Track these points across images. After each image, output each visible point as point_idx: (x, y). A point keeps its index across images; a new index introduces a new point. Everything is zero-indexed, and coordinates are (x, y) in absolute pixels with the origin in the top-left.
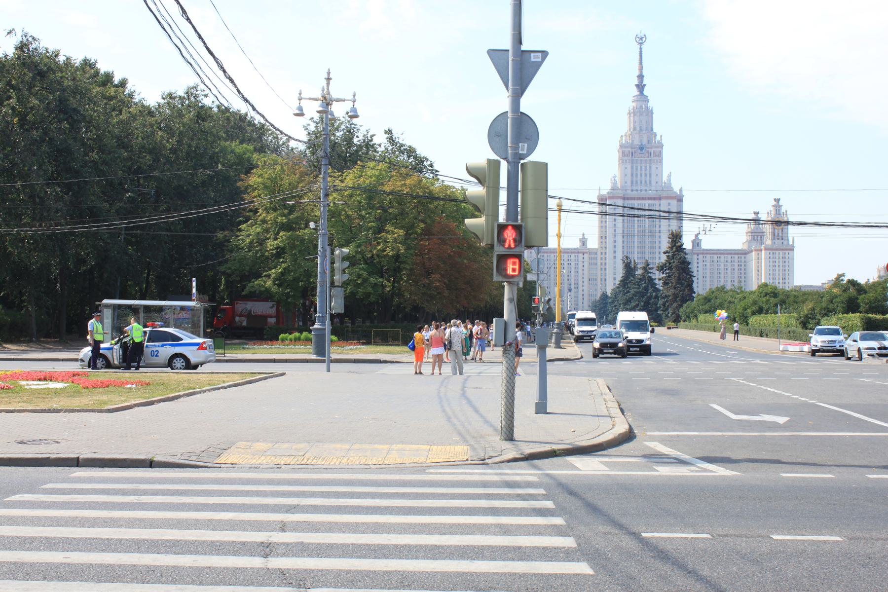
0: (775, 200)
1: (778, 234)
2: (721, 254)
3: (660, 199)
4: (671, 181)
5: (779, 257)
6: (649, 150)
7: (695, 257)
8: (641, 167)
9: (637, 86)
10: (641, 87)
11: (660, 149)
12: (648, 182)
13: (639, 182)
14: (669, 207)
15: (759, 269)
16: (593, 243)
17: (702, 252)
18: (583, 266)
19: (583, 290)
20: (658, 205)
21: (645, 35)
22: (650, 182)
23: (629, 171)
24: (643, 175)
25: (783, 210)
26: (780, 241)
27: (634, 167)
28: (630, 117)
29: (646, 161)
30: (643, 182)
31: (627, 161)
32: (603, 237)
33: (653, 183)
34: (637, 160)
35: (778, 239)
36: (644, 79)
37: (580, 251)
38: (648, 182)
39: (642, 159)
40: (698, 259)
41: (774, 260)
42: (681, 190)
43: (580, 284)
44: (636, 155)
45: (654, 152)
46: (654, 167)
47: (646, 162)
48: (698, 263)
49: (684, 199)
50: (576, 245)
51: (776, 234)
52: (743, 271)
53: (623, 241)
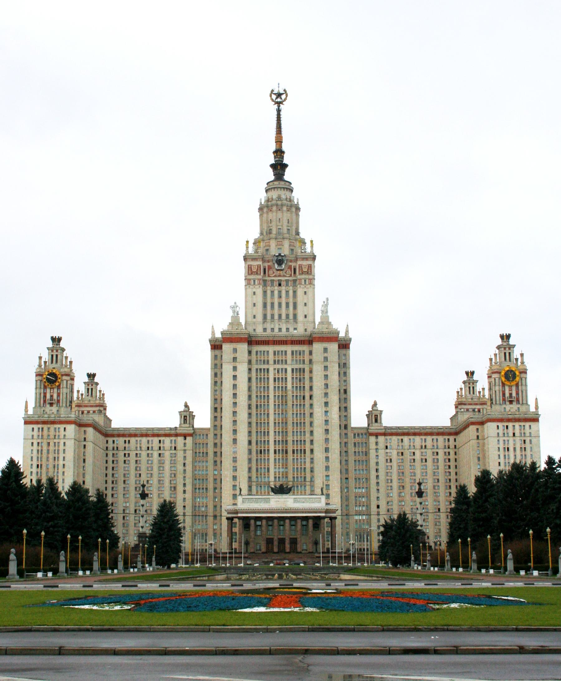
0: (502, 337)
1: (511, 394)
2: (415, 434)
4: (329, 314)
5: (514, 434)
6: (293, 264)
7: (372, 439)
8: (280, 292)
9: (273, 166)
11: (310, 262)
12: (291, 317)
13: (276, 317)
14: (326, 355)
15: (481, 456)
18: (185, 457)
19: (184, 499)
20: (307, 353)
21: (285, 90)
22: (295, 316)
24: (284, 305)
25: (516, 353)
26: (514, 406)
27: (269, 293)
28: (261, 215)
29: (287, 281)
30: (284, 317)
31: (256, 281)
32: (217, 409)
33: (300, 318)
34: (272, 281)
35: (511, 402)
36: (285, 156)
38: (291, 317)
39: (280, 278)
40: (377, 443)
41: (506, 439)
42: (347, 332)
43: (180, 488)
44: (271, 272)
45: (300, 266)
46: (300, 292)
47: (287, 285)
50: (174, 422)
51: (507, 395)
52: (452, 464)
53: (250, 414)
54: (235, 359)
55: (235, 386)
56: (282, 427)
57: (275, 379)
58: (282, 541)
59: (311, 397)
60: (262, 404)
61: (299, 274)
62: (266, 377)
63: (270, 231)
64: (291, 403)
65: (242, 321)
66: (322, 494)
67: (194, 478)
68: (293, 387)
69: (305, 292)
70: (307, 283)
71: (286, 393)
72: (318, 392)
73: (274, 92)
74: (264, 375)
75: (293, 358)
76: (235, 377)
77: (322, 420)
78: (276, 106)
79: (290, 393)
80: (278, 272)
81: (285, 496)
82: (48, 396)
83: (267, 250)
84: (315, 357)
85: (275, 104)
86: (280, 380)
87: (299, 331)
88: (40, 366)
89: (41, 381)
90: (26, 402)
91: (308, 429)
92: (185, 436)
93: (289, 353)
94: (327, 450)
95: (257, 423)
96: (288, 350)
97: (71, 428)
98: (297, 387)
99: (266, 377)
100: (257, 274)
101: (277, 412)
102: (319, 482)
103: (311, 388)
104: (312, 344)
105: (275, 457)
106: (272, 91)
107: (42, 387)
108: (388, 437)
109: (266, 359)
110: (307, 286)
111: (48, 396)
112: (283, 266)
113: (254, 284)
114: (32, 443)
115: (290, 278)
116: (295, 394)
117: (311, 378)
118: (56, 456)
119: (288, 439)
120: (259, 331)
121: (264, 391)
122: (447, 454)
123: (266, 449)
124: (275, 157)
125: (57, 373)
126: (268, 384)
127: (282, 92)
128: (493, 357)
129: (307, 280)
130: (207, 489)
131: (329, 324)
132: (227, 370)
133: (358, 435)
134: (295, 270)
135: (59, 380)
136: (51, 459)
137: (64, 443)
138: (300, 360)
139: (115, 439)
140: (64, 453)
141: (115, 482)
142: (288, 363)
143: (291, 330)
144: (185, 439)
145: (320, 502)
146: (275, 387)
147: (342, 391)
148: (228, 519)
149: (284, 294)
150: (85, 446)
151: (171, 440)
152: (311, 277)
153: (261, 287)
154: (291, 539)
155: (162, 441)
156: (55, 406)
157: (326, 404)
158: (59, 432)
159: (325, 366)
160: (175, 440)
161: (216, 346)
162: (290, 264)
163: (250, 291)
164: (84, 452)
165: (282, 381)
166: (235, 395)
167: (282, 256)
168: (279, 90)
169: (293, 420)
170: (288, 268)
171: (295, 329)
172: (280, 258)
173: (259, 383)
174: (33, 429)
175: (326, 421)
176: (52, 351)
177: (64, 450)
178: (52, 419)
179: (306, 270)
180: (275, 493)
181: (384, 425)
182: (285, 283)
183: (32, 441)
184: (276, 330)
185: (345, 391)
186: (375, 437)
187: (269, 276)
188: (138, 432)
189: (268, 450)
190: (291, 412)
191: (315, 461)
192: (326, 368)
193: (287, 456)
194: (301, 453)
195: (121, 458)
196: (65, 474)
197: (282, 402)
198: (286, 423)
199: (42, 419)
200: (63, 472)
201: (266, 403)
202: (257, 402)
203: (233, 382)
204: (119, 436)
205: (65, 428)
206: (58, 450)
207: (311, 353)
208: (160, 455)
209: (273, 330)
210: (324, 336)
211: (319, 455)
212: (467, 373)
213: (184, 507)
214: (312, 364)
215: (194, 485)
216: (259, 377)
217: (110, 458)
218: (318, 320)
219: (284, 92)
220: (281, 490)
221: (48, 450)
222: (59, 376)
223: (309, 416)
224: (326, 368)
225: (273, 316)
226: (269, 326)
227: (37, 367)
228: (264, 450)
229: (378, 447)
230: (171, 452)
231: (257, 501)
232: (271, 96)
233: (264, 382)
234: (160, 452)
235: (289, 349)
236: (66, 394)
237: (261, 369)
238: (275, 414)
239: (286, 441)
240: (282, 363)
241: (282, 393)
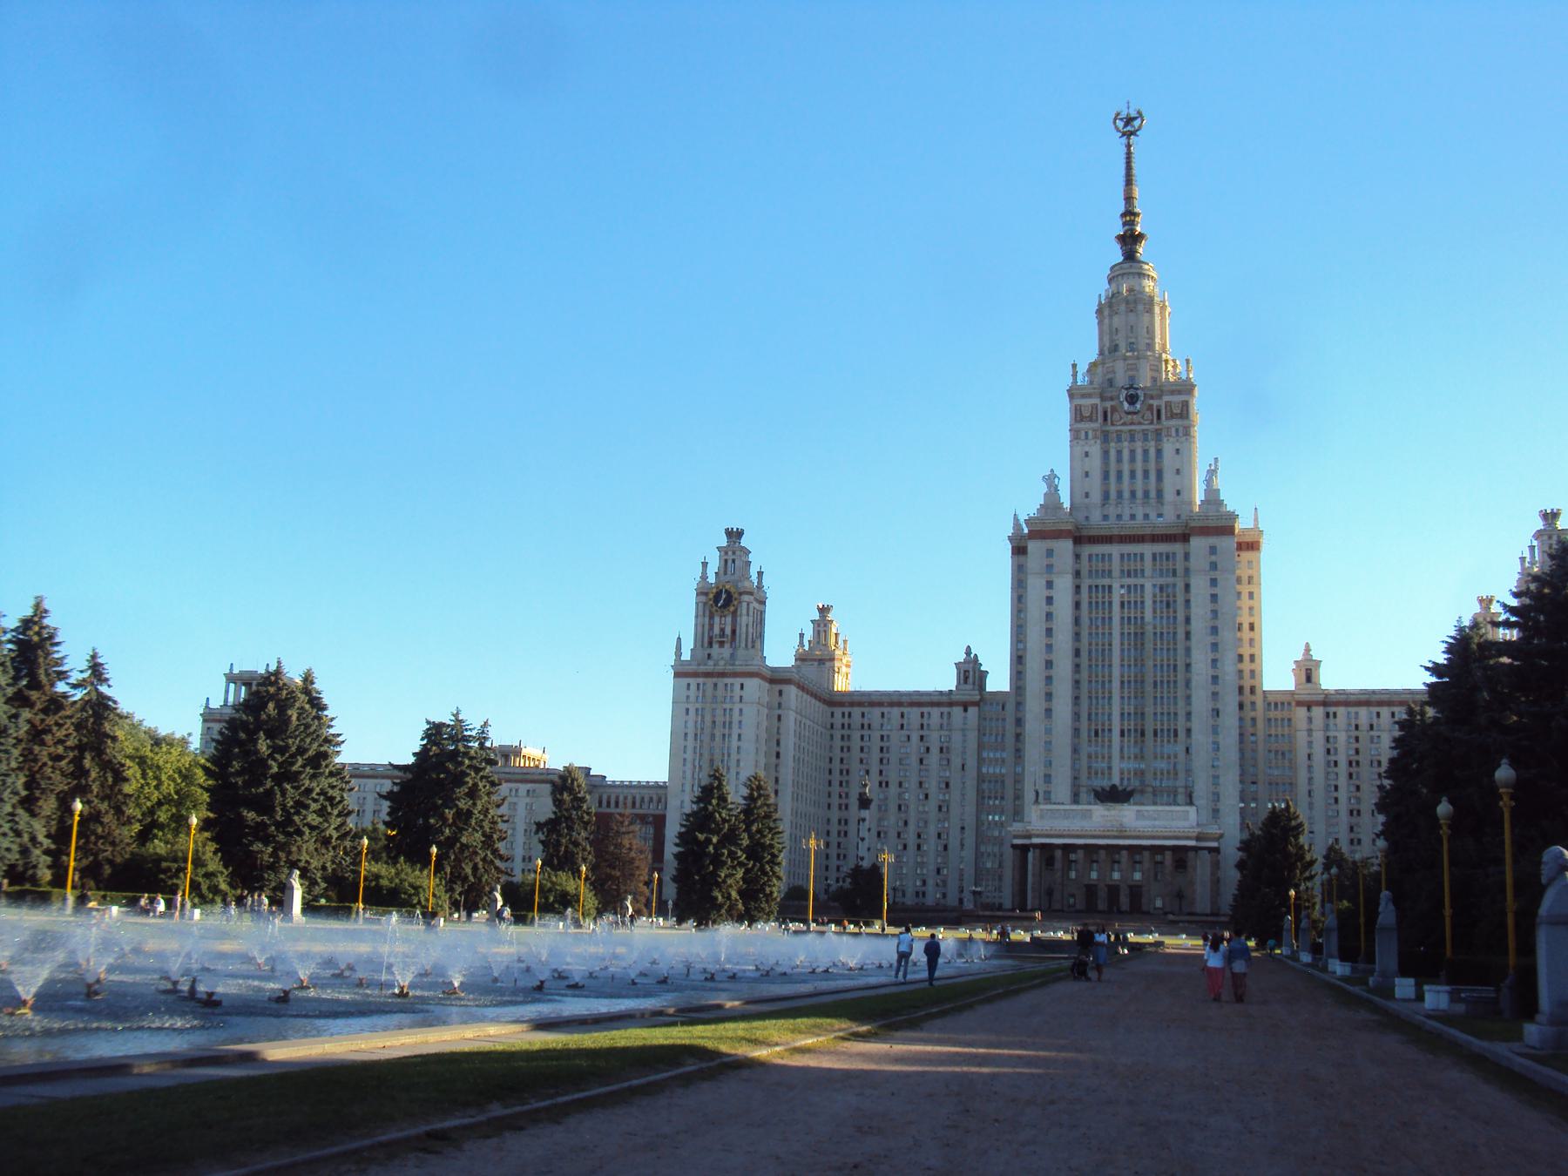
3: (1185, 538)
6: (1155, 403)
7: (1301, 713)
8: (1132, 452)
10: (1130, 240)
12: (1153, 494)
13: (1126, 495)
14: (1213, 558)
16: (999, 680)
17: (1320, 698)
20: (1180, 557)
21: (1140, 115)
22: (1160, 494)
23: (1095, 463)
27: (1113, 453)
28: (1100, 323)
29: (1145, 434)
30: (1139, 494)
32: (1018, 660)
33: (1169, 495)
37: (955, 698)
39: (1133, 427)
40: (1310, 720)
42: (1256, 519)
44: (1116, 416)
45: (1168, 404)
46: (1168, 447)
47: (1146, 439)
48: (1310, 731)
49: (1264, 547)
50: (945, 680)
54: (1050, 567)
55: (1049, 616)
56: (1136, 688)
57: (1122, 604)
58: (1113, 890)
59: (1188, 635)
60: (1100, 647)
61: (1167, 418)
62: (1107, 599)
63: (1115, 348)
64: (1152, 646)
65: (1066, 501)
66: (1191, 803)
67: (981, 779)
68: (1155, 618)
69: (1178, 451)
70: (1181, 434)
71: (1142, 628)
72: (1199, 625)
74: (1103, 597)
75: (1155, 565)
76: (1050, 600)
77: (1207, 675)
78: (1124, 140)
79: (1149, 629)
80: (1130, 416)
81: (1118, 806)
82: (717, 630)
83: (1111, 382)
84: (1194, 563)
85: (1124, 134)
86: (1132, 604)
87: (1167, 519)
88: (704, 577)
89: (705, 604)
90: (679, 639)
91: (1181, 692)
92: (965, 706)
94: (1215, 730)
95: (1090, 682)
96: (1145, 552)
97: (754, 687)
98: (1162, 618)
99: (1107, 599)
100: (1091, 420)
101: (1126, 663)
102: (1201, 788)
103: (1188, 620)
104: (1189, 541)
105: (1122, 741)
106: (1118, 114)
107: (707, 613)
108: (1332, 710)
109: (1107, 568)
110: (1180, 440)
111: (717, 630)
112: (1138, 406)
113: (1087, 437)
114: (687, 710)
115: (1151, 427)
116: (1158, 631)
117: (1188, 602)
118: (727, 732)
119: (1147, 710)
120: (1096, 517)
121: (1103, 624)
123: (1106, 728)
124: (1124, 224)
125: (732, 590)
126: (1110, 612)
127: (1133, 114)
128: (1527, 554)
129: (1181, 429)
131: (1220, 503)
132: (1036, 586)
133: (1276, 704)
134: (1159, 412)
135: (736, 603)
136: (718, 738)
137: (741, 710)
138: (1168, 570)
139: (846, 710)
140: (740, 728)
141: (844, 784)
142: (1146, 575)
143: (1153, 516)
144: (966, 710)
145: (1186, 819)
146: (1122, 618)
148: (1014, 847)
149: (1139, 457)
150: (779, 718)
151: (942, 713)
152: (1186, 422)
153: (1099, 441)
154: (1131, 887)
155: (925, 714)
156: (727, 645)
157: (1215, 646)
158: (732, 691)
159: (1211, 579)
160: (949, 713)
161: (1019, 550)
162: (1151, 402)
163: (1078, 449)
164: (778, 728)
165: (1136, 607)
166: (1049, 632)
167: (1137, 389)
169: (1155, 676)
170: (1148, 409)
171: (1160, 515)
172: (1132, 392)
173: (1094, 611)
174: (689, 685)
175: (1215, 679)
176: (726, 553)
177: (740, 722)
178: (720, 668)
179: (1179, 411)
180: (1102, 801)
181: (1323, 687)
182: (1141, 435)
184: (1126, 517)
187: (1112, 424)
188: (885, 699)
189: (1110, 730)
190: (1151, 663)
191: (1193, 750)
192: (1214, 582)
193: (1143, 741)
194: (1169, 736)
195: (856, 743)
196: (742, 764)
197: (1136, 644)
198: (1143, 682)
199: (702, 669)
200: (738, 761)
201: (1107, 647)
202: (1090, 644)
203: (1046, 608)
204: (852, 704)
205: (742, 686)
206: (730, 723)
207: (1187, 556)
208: (922, 738)
209: (1119, 517)
210: (1212, 524)
211: (1200, 739)
212: (1481, 601)
213: (963, 828)
214: (1189, 577)
215: (980, 792)
216: (1094, 600)
217: (838, 743)
218: (1199, 496)
220: (1113, 796)
221: (714, 722)
222: (736, 596)
223: (1184, 668)
224: (1214, 582)
225: (1120, 494)
226: (1112, 511)
227: (699, 579)
228: (1103, 730)
229: (1313, 727)
230: (943, 733)
231: (1067, 815)
232: (1115, 123)
233: (1103, 609)
234: (921, 733)
235: (1147, 549)
236: (747, 625)
237: (1097, 586)
238: (1122, 666)
239: (1143, 714)
240: (1136, 576)
241: (1136, 628)
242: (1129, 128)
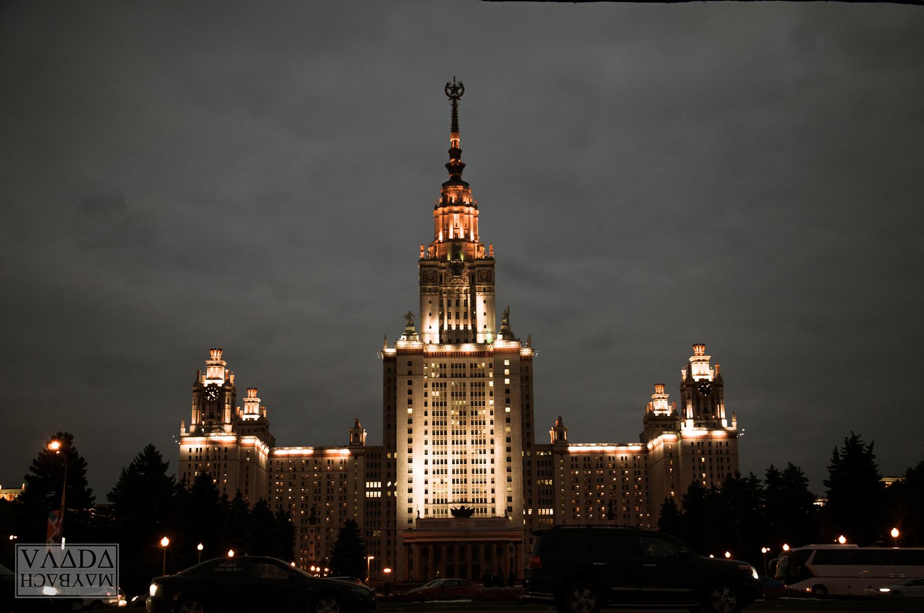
9: (448, 166)
21: (461, 84)
73: (449, 86)
93: (468, 366)
106: (448, 84)
121: (441, 405)
122: (637, 473)
127: (457, 85)
130: (379, 512)
137: (225, 465)
147: (524, 406)
168: (454, 84)
183: (189, 463)
185: (528, 407)
186: (559, 455)
219: (460, 86)
232: (446, 90)
242: (455, 94)
